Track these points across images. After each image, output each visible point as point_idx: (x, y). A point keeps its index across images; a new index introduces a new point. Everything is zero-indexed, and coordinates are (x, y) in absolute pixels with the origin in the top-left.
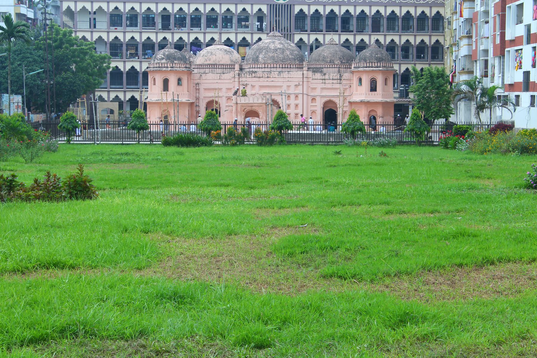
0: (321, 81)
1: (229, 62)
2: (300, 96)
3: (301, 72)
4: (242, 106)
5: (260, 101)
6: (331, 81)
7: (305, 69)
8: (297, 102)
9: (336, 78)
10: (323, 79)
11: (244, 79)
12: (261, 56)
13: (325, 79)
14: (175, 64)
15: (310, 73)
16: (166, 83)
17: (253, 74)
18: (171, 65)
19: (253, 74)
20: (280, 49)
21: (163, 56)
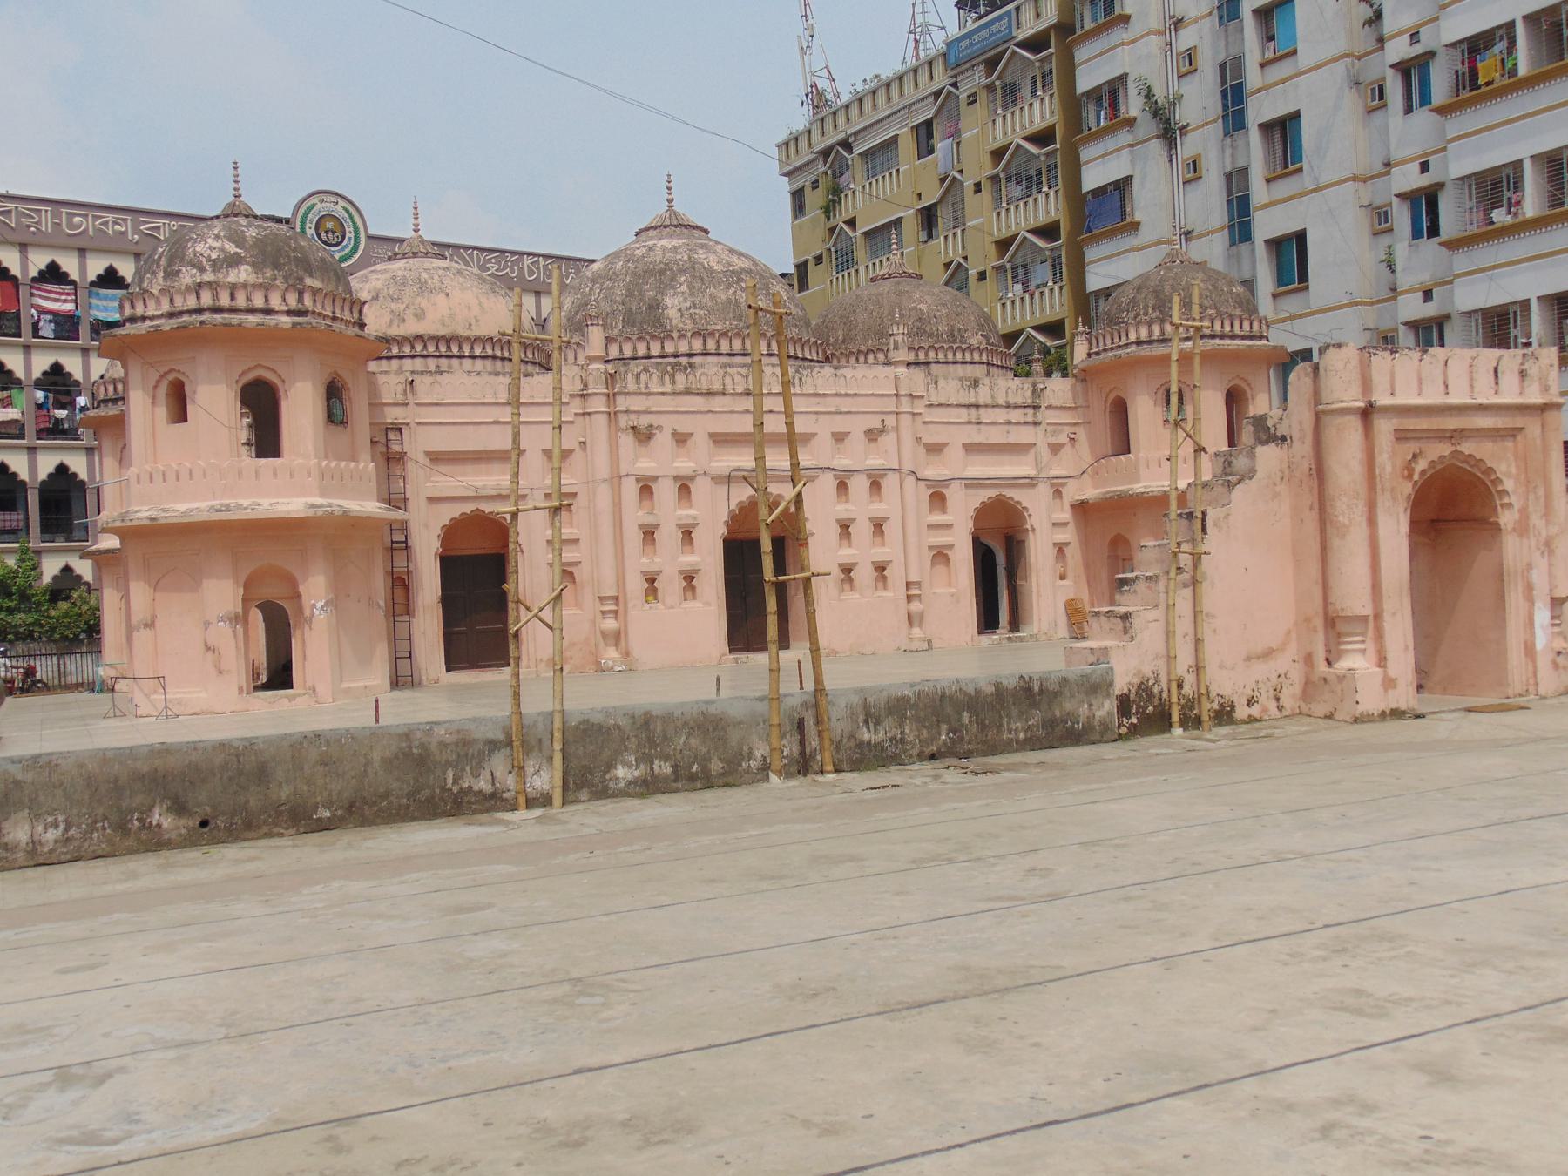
0: (963, 414)
2: (890, 483)
3: (890, 370)
4: (1401, 436)
5: (1510, 394)
6: (1001, 415)
7: (893, 355)
8: (879, 508)
9: (1019, 400)
10: (969, 406)
11: (637, 404)
12: (669, 302)
13: (977, 406)
14: (315, 292)
15: (918, 374)
17: (680, 378)
18: (292, 299)
19: (680, 378)
20: (750, 272)
21: (231, 248)
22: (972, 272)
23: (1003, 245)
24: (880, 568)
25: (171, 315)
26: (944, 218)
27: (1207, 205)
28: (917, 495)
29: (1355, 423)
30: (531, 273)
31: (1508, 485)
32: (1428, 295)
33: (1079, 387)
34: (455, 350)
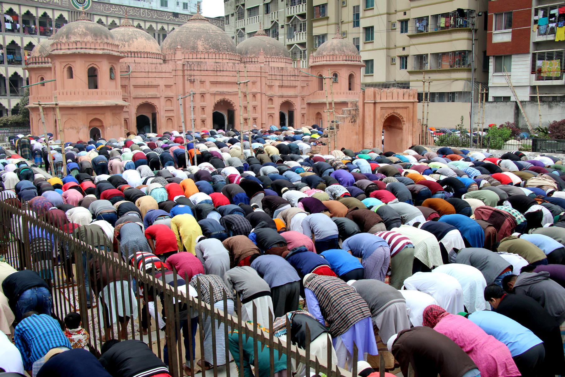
1: (155, 51)
2: (258, 96)
4: (382, 108)
8: (254, 103)
14: (108, 44)
16: (93, 75)
22: (280, 25)
23: (289, 18)
24: (255, 119)
25: (69, 49)
26: (271, 7)
27: (348, 15)
28: (265, 99)
29: (372, 105)
30: (143, 14)
31: (405, 119)
32: (404, 48)
33: (310, 70)
34: (139, 56)
